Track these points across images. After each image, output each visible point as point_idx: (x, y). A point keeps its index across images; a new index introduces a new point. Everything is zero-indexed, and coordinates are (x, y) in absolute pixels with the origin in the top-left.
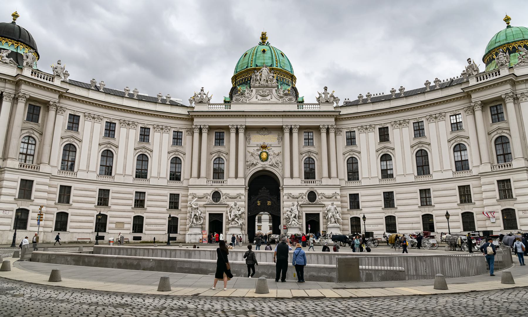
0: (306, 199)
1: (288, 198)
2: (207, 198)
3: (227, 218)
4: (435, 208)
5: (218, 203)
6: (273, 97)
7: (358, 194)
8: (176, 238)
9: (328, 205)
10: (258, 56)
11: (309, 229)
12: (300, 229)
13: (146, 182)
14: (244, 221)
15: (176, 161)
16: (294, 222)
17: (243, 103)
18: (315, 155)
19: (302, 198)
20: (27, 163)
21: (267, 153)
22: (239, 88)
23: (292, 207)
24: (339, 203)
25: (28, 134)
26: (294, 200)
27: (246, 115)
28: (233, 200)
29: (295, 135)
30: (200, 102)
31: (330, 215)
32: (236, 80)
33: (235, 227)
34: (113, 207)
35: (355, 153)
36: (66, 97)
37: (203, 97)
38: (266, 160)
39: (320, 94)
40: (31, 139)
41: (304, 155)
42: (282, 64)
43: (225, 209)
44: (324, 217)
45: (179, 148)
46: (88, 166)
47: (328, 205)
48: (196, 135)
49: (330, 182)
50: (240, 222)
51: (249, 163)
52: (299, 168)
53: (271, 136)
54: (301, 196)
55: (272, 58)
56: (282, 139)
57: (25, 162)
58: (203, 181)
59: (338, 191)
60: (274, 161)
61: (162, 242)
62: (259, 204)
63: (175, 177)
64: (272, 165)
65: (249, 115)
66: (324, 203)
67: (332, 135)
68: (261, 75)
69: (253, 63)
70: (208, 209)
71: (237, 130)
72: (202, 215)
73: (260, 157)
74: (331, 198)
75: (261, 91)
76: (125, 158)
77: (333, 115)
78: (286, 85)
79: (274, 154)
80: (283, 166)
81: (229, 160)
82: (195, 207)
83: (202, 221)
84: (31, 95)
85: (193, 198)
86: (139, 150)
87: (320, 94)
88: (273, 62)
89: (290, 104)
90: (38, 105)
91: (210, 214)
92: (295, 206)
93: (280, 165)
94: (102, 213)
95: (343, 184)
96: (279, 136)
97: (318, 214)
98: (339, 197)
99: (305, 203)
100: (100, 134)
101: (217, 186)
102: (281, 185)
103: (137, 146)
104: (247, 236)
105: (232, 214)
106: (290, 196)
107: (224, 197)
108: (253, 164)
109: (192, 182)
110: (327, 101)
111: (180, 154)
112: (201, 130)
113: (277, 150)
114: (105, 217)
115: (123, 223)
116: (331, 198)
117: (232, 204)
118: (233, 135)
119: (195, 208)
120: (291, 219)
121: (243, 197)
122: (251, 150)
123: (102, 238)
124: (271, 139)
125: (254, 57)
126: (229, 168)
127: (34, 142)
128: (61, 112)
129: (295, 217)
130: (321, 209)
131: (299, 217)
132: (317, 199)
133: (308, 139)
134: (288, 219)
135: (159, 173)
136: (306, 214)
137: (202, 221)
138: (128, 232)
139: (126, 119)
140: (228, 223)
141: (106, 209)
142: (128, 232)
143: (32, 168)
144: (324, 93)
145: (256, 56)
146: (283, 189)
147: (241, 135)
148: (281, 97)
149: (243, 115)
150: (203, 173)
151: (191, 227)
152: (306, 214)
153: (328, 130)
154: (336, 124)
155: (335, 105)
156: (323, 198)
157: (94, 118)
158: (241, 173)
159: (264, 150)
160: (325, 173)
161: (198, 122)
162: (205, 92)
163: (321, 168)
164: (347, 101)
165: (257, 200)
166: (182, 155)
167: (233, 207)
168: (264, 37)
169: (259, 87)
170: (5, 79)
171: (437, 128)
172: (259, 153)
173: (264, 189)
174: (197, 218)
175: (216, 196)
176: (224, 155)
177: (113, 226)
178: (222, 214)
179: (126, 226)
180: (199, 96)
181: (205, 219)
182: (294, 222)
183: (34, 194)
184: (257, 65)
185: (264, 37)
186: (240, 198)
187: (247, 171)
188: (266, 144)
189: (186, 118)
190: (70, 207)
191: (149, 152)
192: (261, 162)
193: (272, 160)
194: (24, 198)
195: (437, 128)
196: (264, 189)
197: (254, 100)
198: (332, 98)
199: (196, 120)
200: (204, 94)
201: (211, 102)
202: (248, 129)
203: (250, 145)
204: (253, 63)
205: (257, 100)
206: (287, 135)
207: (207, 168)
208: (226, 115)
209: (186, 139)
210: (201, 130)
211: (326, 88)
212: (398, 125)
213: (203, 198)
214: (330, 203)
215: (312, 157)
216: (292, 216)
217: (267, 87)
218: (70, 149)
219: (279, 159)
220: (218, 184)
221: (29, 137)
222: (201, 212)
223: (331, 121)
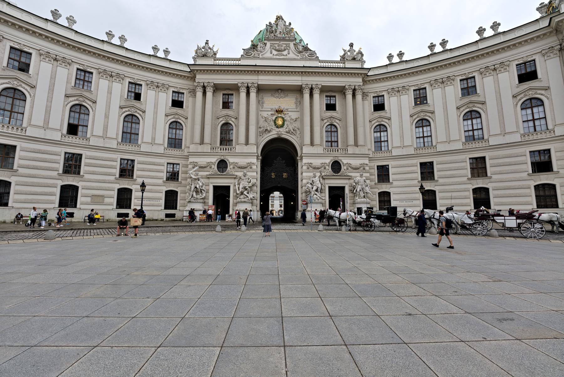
1: (308, 168)
2: (211, 168)
3: (235, 191)
4: (491, 180)
6: (291, 52)
8: (175, 214)
9: (356, 177)
11: (341, 203)
12: (323, 204)
13: (136, 148)
14: (256, 194)
15: (175, 125)
17: (255, 58)
18: (337, 121)
19: (325, 168)
21: (283, 118)
23: (314, 179)
27: (258, 71)
28: (242, 170)
29: (316, 96)
31: (359, 188)
33: (245, 202)
34: (87, 176)
35: (384, 120)
38: (282, 126)
39: (345, 51)
41: (325, 121)
43: (232, 181)
44: (351, 191)
47: (356, 177)
48: (199, 94)
49: (357, 150)
50: (251, 196)
51: (261, 129)
52: (320, 134)
53: (287, 99)
54: (323, 165)
56: (300, 103)
58: (206, 148)
59: (366, 161)
61: (157, 220)
62: (273, 177)
63: (175, 143)
64: (288, 132)
65: (262, 71)
67: (359, 97)
70: (211, 180)
71: (248, 88)
72: (203, 188)
73: (275, 122)
74: (358, 169)
75: (276, 45)
76: (107, 116)
77: (361, 74)
79: (292, 119)
81: (238, 126)
82: (194, 177)
83: (204, 195)
86: (127, 109)
87: (345, 51)
91: (215, 188)
92: (317, 178)
93: (298, 132)
96: (296, 99)
99: (328, 174)
100: (68, 82)
101: (223, 153)
102: (299, 155)
103: (123, 104)
104: (259, 213)
105: (241, 186)
106: (310, 165)
107: (232, 167)
108: (266, 130)
109: (193, 148)
111: (181, 117)
112: (204, 87)
113: (294, 115)
115: (103, 196)
116: (358, 169)
117: (240, 174)
118: (243, 95)
119: (195, 179)
120: (313, 193)
121: (254, 167)
122: (265, 114)
123: (71, 215)
124: (287, 103)
126: (238, 134)
129: (317, 190)
130: (347, 181)
131: (322, 191)
132: (342, 170)
134: (308, 192)
135: (153, 139)
137: (204, 195)
138: (110, 207)
140: (236, 197)
142: (110, 207)
144: (349, 51)
146: (301, 159)
147: (253, 95)
148: (300, 52)
149: (255, 71)
150: (207, 139)
151: (189, 202)
152: (330, 187)
153: (354, 91)
156: (350, 169)
157: (56, 60)
158: (252, 139)
159: (280, 115)
161: (200, 78)
162: (211, 46)
165: (271, 172)
167: (243, 178)
169: (274, 40)
171: (497, 83)
172: (274, 118)
173: (279, 159)
174: (197, 191)
175: (222, 165)
176: (233, 120)
177: (89, 199)
178: (229, 186)
179: (107, 200)
181: (207, 192)
182: (316, 196)
186: (251, 168)
187: (260, 138)
188: (282, 108)
189: (188, 77)
191: (141, 113)
192: (276, 128)
193: (289, 126)
195: (497, 83)
196: (279, 159)
197: (268, 55)
198: (360, 55)
201: (218, 56)
202: (261, 89)
203: (263, 109)
205: (271, 55)
206: (307, 96)
207: (212, 134)
208: (235, 71)
209: (187, 99)
210: (204, 87)
211: (351, 45)
212: (439, 84)
213: (205, 167)
214: (358, 174)
215: (335, 124)
217: (284, 39)
219: (297, 125)
222: (203, 184)
223: (358, 81)
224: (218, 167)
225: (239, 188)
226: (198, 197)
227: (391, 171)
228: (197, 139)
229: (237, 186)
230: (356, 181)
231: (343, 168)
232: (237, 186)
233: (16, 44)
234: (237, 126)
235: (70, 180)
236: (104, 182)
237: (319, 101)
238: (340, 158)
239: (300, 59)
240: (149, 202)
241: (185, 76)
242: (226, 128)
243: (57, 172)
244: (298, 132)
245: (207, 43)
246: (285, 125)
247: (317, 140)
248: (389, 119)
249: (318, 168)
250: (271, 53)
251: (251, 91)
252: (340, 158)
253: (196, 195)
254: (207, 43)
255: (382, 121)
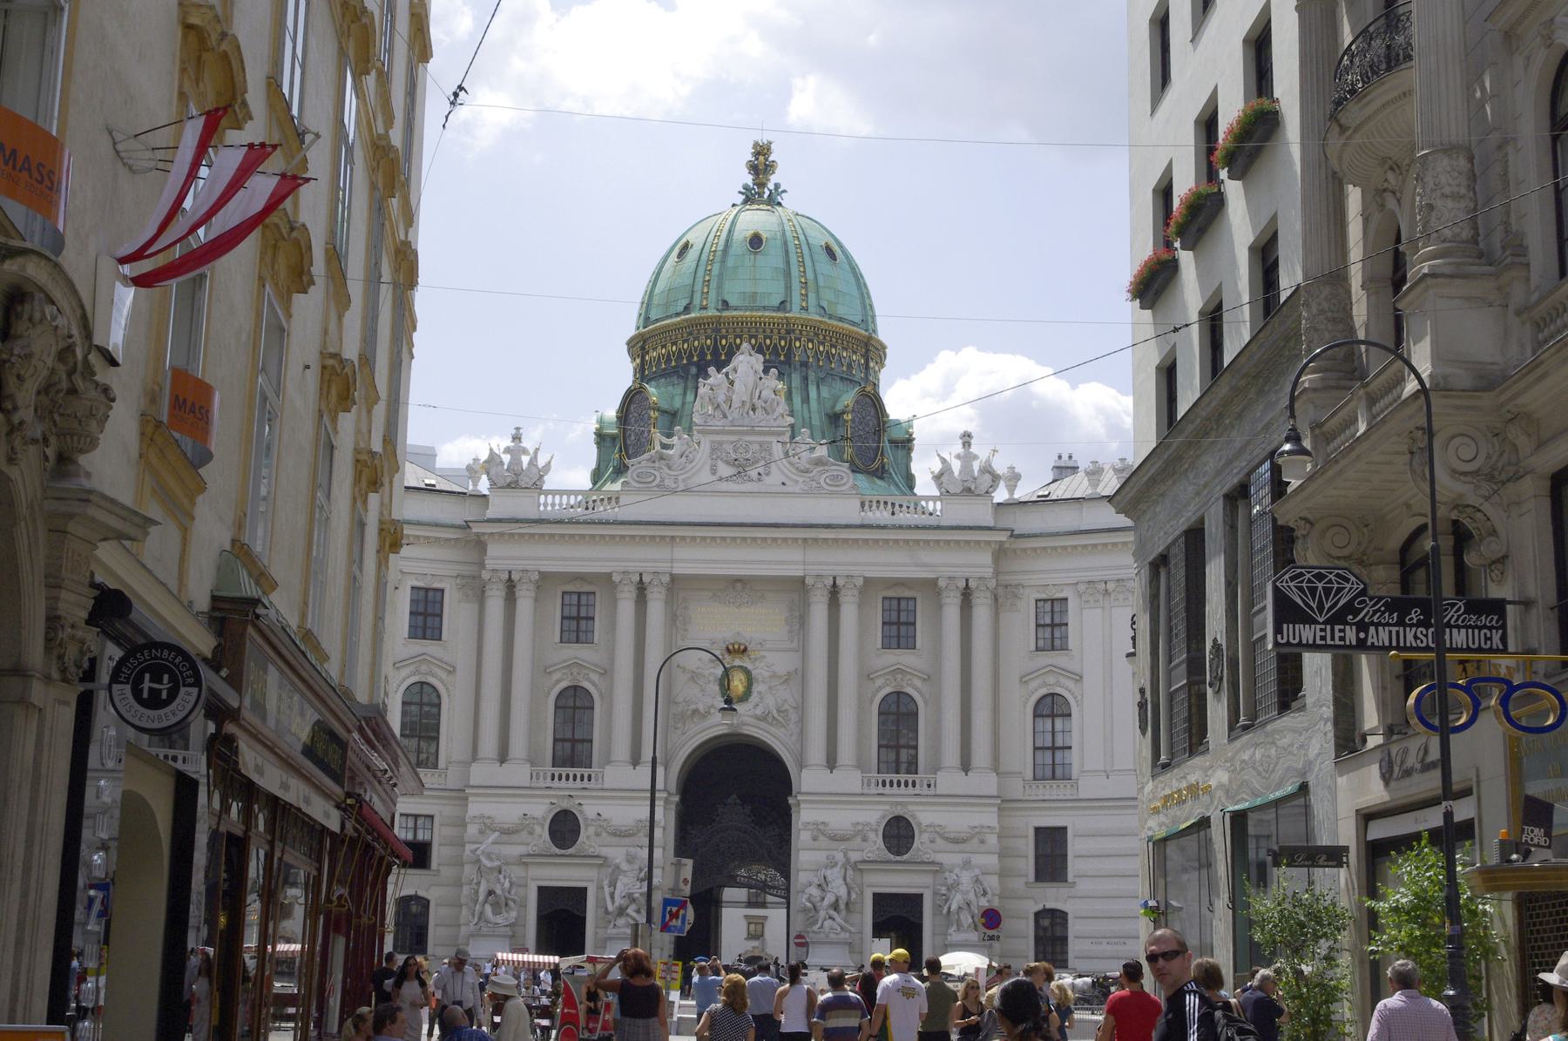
0: (875, 846)
2: (531, 833)
5: (570, 851)
7: (1064, 829)
10: (730, 262)
16: (831, 925)
17: (664, 490)
19: (865, 839)
21: (748, 673)
22: (652, 390)
23: (828, 872)
24: (992, 861)
26: (834, 845)
30: (509, 486)
32: (644, 351)
37: (520, 463)
39: (944, 461)
42: (827, 296)
44: (937, 908)
45: (429, 647)
52: (858, 729)
54: (860, 832)
55: (788, 274)
56: (801, 621)
58: (517, 772)
59: (989, 818)
60: (770, 702)
64: (763, 718)
66: (939, 858)
67: (982, 613)
68: (732, 383)
69: (713, 295)
70: (534, 872)
71: (641, 588)
75: (729, 448)
77: (988, 543)
78: (838, 385)
79: (774, 676)
80: (802, 721)
82: (488, 864)
83: (514, 914)
85: (481, 832)
87: (944, 461)
88: (788, 288)
89: (832, 493)
91: (540, 888)
92: (837, 869)
95: (1016, 789)
97: (918, 898)
98: (992, 840)
99: (872, 857)
101: (564, 792)
106: (819, 830)
107: (591, 830)
110: (969, 490)
111: (435, 670)
112: (511, 586)
116: (964, 841)
119: (491, 869)
120: (822, 914)
124: (759, 624)
125: (716, 268)
126: (613, 725)
129: (835, 906)
133: (899, 624)
136: (879, 899)
145: (723, 262)
146: (798, 804)
152: (879, 899)
153: (967, 594)
154: (997, 573)
155: (1001, 495)
156: (939, 840)
159: (737, 662)
160: (951, 753)
162: (527, 443)
163: (939, 729)
164: (1065, 461)
166: (443, 675)
167: (624, 866)
168: (761, 163)
174: (498, 902)
180: (506, 458)
181: (523, 906)
182: (831, 925)
184: (725, 303)
185: (761, 163)
193: (766, 697)
198: (988, 477)
199: (493, 550)
200: (525, 451)
201: (550, 482)
202: (677, 584)
204: (713, 295)
207: (532, 724)
209: (456, 614)
210: (511, 586)
216: (826, 902)
220: (571, 783)
222: (511, 884)
223: (978, 564)
224: (553, 833)
225: (612, 896)
226: (499, 920)
227: (1074, 846)
228: (489, 745)
229: (607, 890)
230: (950, 882)
231: (920, 840)
232: (607, 890)
234: (609, 697)
237: (858, 624)
238: (911, 808)
239: (806, 494)
241: (447, 540)
242: (574, 706)
244: (794, 716)
245: (517, 438)
246: (755, 694)
247: (846, 751)
248: (1079, 678)
249: (843, 839)
250: (714, 471)
251: (649, 596)
252: (911, 808)
253: (495, 913)
254: (517, 438)
255: (1058, 684)
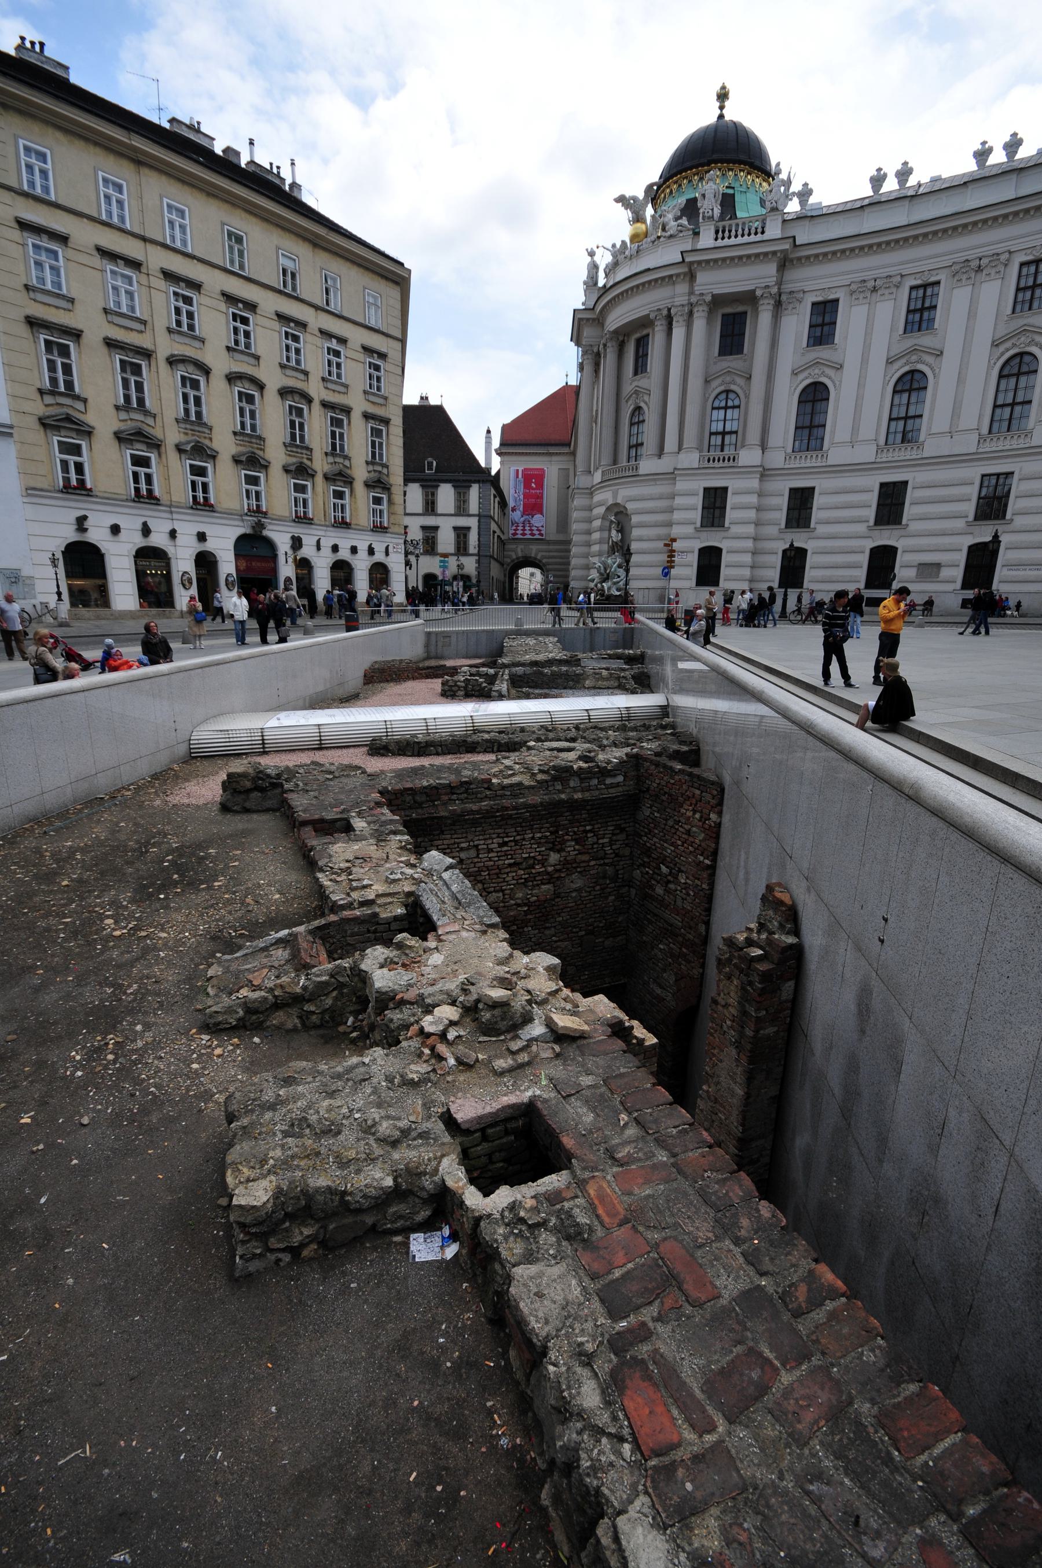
20: (726, 452)
25: (722, 388)
36: (799, 259)
40: (731, 396)
46: (855, 429)
57: (722, 450)
76: (961, 380)
84: (716, 292)
90: (740, 309)
94: (796, 544)
114: (802, 553)
115: (938, 566)
127: (736, 403)
128: (791, 306)
138: (950, 587)
139: (971, 254)
141: (895, 532)
142: (950, 587)
143: (724, 460)
170: (671, 276)
179: (945, 573)
183: (730, 515)
190: (813, 535)
194: (713, 526)
218: (814, 396)
221: (727, 392)
233: (818, 293)
235: (886, 537)
236: (944, 534)
240: (1036, 573)
243: (866, 524)
